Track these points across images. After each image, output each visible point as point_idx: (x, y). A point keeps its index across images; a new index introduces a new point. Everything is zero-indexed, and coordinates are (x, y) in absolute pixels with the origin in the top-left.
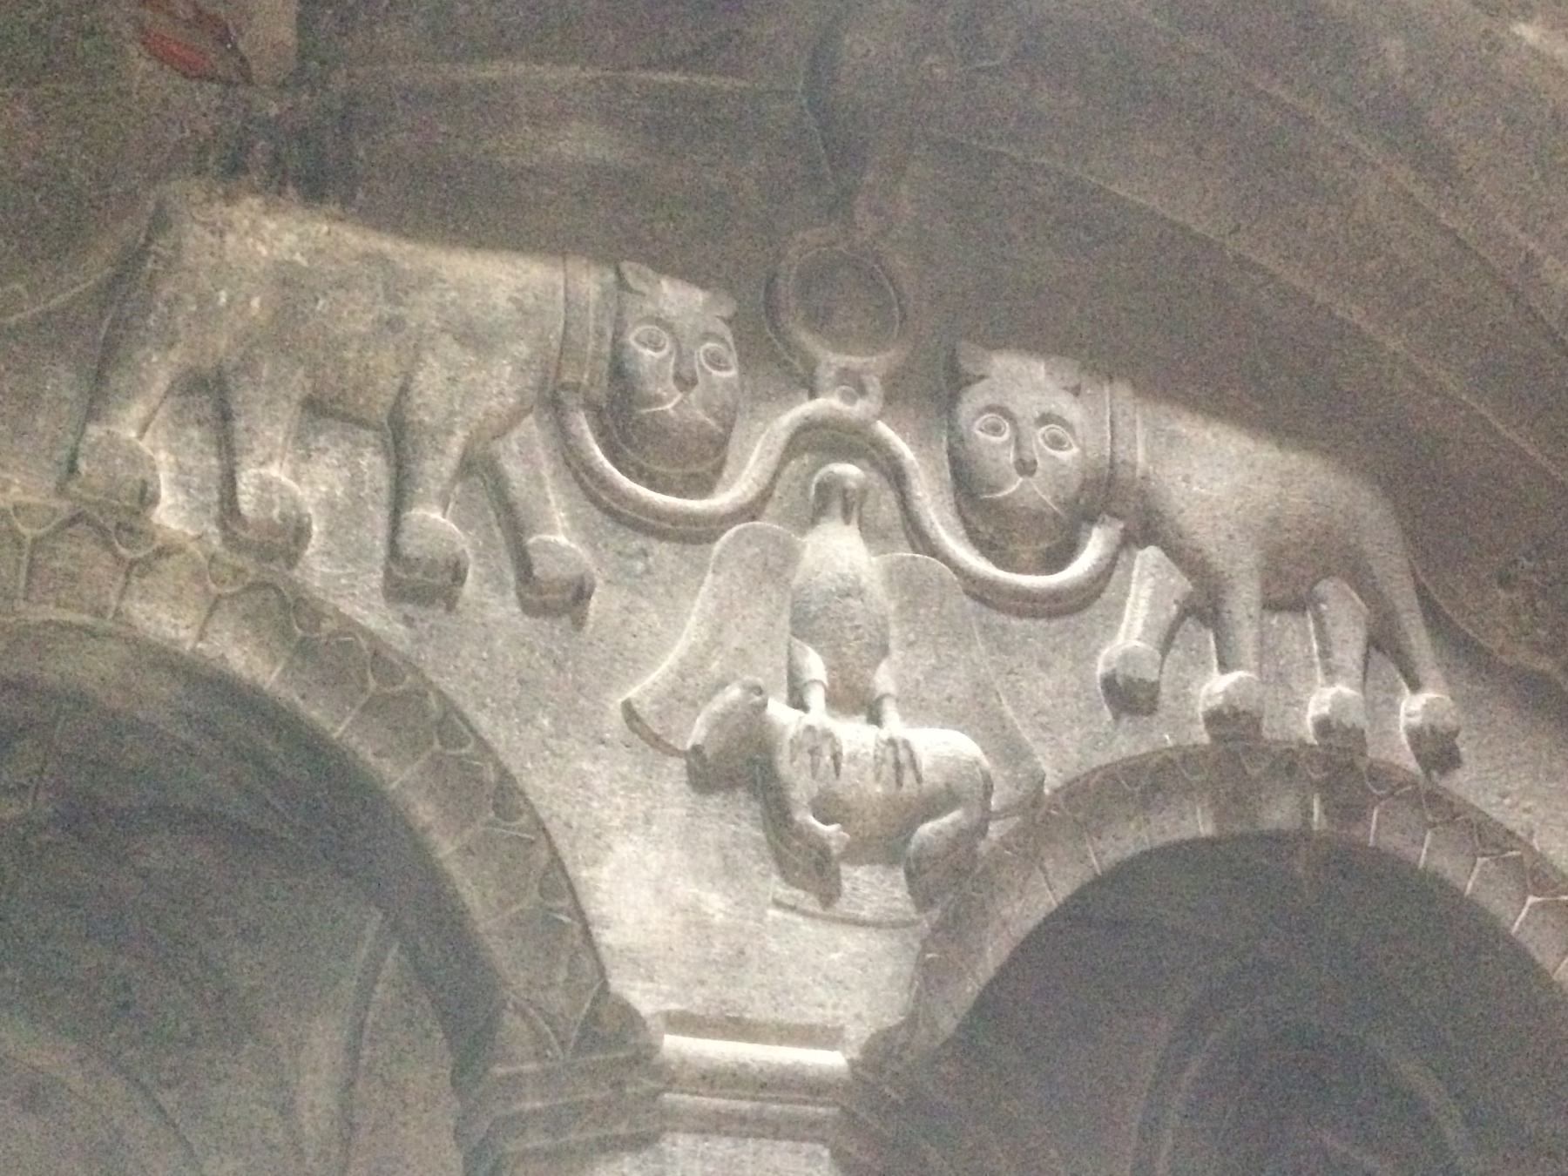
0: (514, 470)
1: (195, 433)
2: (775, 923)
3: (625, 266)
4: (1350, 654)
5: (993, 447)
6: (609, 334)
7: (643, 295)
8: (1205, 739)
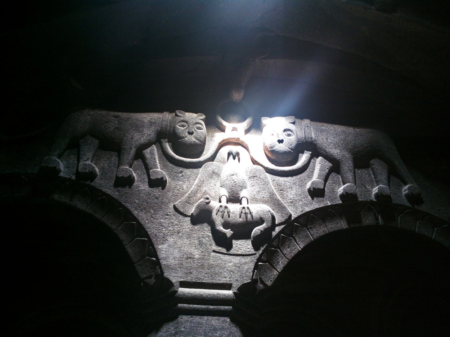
0: (148, 156)
1: (72, 157)
3: (177, 111)
4: (383, 176)
7: (181, 116)
8: (341, 202)
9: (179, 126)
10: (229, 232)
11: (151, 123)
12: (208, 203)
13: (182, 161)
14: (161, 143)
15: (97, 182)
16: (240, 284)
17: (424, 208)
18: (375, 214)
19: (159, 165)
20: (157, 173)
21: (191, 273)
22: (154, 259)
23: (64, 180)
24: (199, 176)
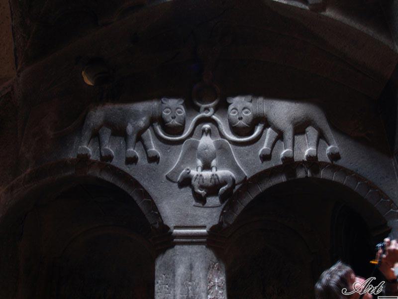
11: (144, 112)
12: (189, 173)
14: (153, 126)
15: (115, 162)
17: (340, 163)
18: (305, 171)
23: (94, 162)
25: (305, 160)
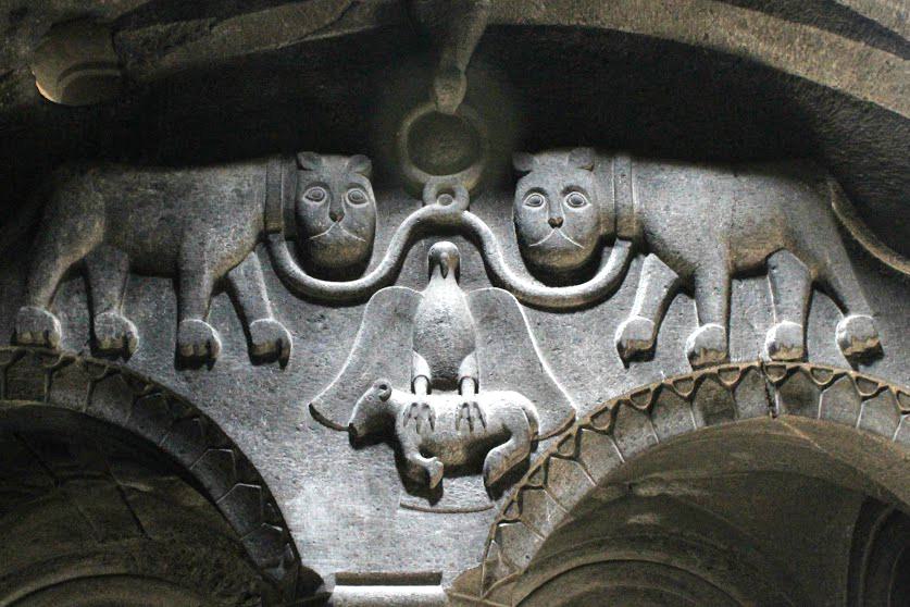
0: (242, 285)
1: (76, 299)
2: (401, 518)
3: (302, 157)
5: (535, 216)
6: (293, 198)
7: (310, 170)
9: (307, 197)
10: (432, 464)
12: (385, 398)
13: (321, 291)
15: (139, 360)
16: (457, 572)
18: (767, 390)
19: (269, 309)
20: (266, 328)
21: (356, 555)
22: (279, 529)
24: (363, 326)
25: (767, 358)
